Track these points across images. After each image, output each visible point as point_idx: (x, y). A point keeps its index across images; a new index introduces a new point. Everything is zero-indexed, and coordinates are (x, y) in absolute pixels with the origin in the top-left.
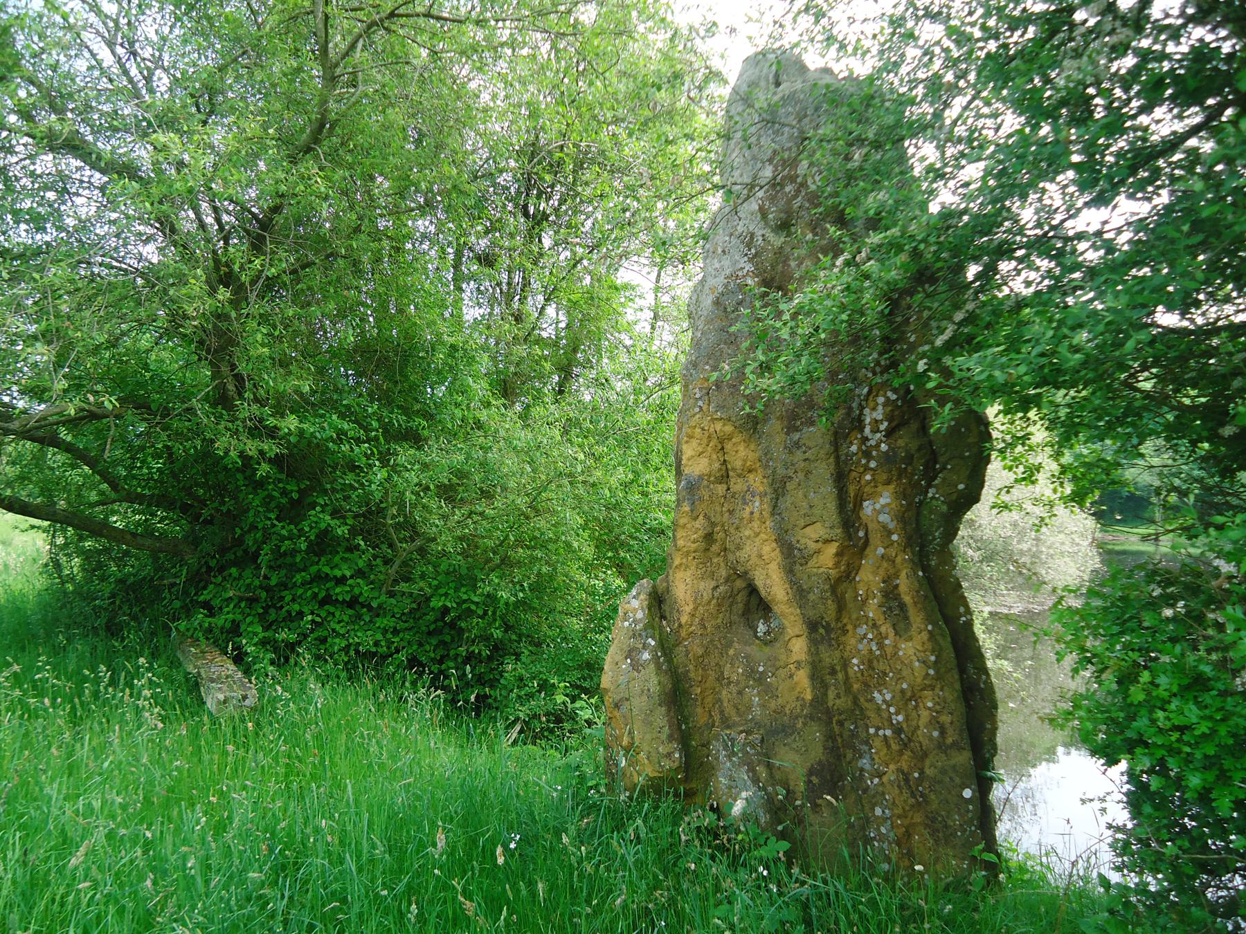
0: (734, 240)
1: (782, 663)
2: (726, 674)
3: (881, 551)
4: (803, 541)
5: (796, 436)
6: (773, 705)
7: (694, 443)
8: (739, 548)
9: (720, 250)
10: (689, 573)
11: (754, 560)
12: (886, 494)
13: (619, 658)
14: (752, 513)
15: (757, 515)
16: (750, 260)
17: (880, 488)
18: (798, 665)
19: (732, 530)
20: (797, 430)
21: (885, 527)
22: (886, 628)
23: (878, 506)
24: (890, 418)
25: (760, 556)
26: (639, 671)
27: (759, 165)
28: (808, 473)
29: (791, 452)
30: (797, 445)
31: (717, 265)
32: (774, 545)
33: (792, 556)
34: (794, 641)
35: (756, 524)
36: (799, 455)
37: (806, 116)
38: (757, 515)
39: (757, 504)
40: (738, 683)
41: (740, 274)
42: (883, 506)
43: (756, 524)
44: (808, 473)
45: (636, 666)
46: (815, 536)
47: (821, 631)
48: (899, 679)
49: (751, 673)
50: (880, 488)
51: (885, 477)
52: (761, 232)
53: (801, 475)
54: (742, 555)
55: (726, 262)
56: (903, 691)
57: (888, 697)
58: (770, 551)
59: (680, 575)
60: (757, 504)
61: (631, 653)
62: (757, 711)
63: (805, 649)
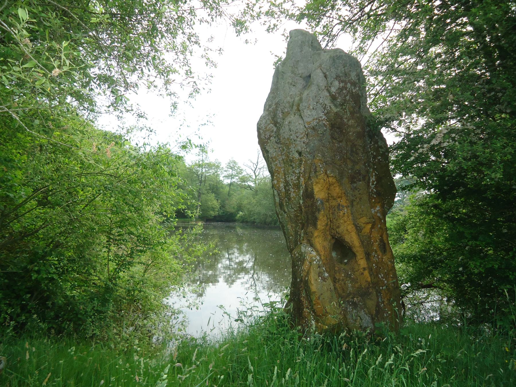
0: (319, 105)
1: (356, 270)
2: (337, 278)
3: (379, 226)
4: (360, 224)
5: (355, 185)
6: (357, 285)
7: (319, 186)
8: (338, 227)
9: (311, 107)
10: (320, 239)
11: (345, 232)
12: (378, 206)
13: (316, 277)
14: (344, 214)
15: (346, 214)
16: (325, 115)
17: (376, 204)
18: (364, 269)
19: (335, 221)
20: (355, 183)
21: (379, 217)
22: (379, 252)
23: (376, 211)
24: (377, 180)
25: (347, 230)
26: (326, 282)
27: (333, 79)
28: (360, 199)
29: (354, 191)
30: (356, 188)
31: (310, 113)
32: (353, 226)
33: (359, 229)
34: (360, 260)
35: (345, 218)
36: (357, 192)
37: (346, 66)
38: (346, 214)
39: (346, 210)
40: (343, 280)
41: (320, 119)
42: (378, 211)
43: (345, 218)
44: (360, 199)
45: (324, 279)
46: (364, 222)
47: (368, 256)
48: (384, 269)
49: (348, 276)
50: (376, 204)
51: (378, 201)
52: (329, 105)
53: (358, 199)
54: (340, 230)
55: (314, 113)
56: (386, 273)
57: (382, 275)
58: (351, 227)
59: (317, 240)
60: (346, 210)
61: (320, 274)
62: (350, 289)
63: (366, 263)
